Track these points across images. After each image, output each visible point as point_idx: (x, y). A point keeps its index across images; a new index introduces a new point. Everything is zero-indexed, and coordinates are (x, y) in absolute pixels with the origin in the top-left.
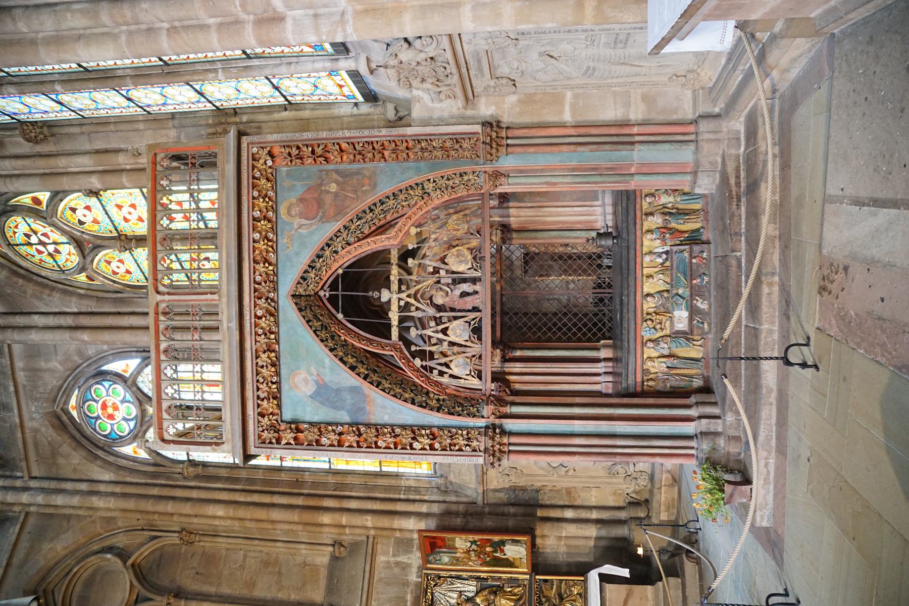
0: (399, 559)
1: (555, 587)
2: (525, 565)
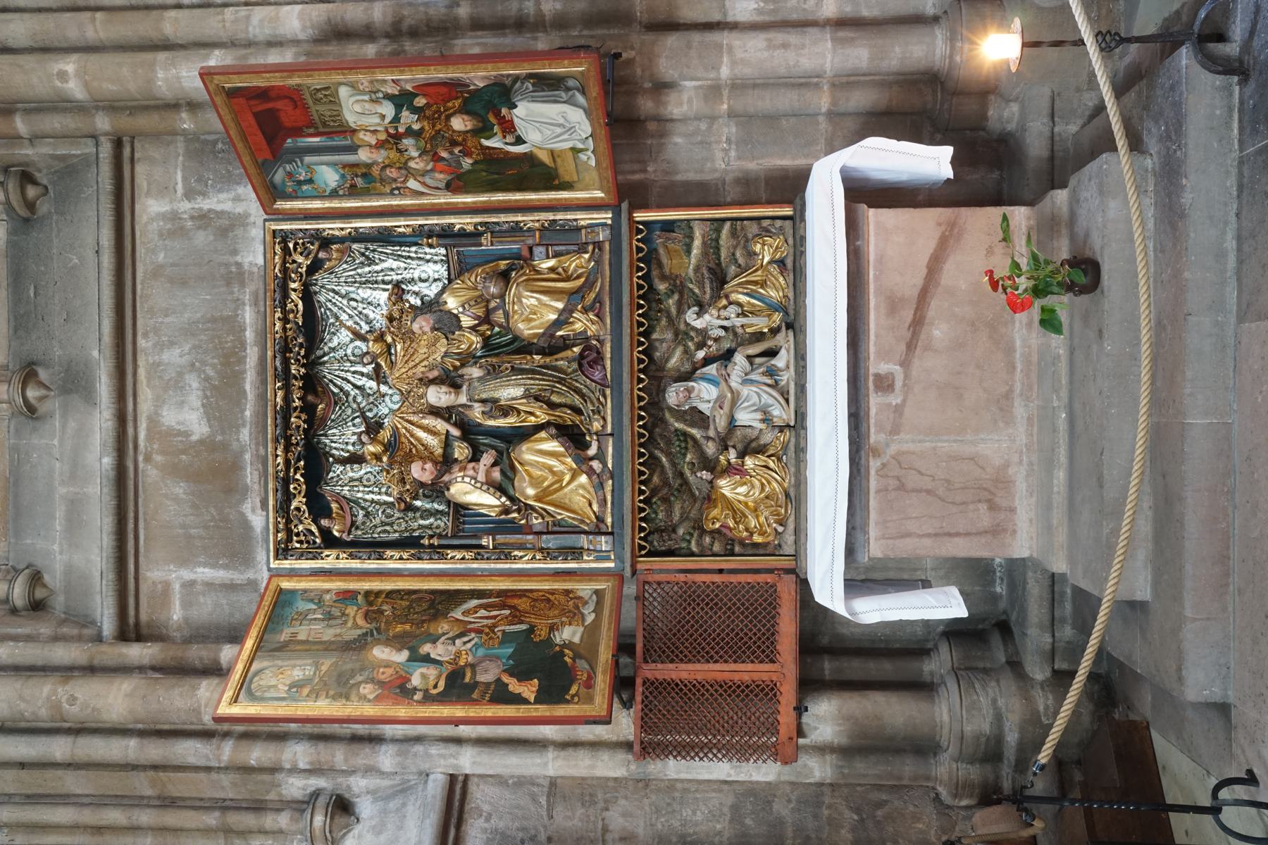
0: (206, 204)
1: (697, 243)
2: (595, 175)
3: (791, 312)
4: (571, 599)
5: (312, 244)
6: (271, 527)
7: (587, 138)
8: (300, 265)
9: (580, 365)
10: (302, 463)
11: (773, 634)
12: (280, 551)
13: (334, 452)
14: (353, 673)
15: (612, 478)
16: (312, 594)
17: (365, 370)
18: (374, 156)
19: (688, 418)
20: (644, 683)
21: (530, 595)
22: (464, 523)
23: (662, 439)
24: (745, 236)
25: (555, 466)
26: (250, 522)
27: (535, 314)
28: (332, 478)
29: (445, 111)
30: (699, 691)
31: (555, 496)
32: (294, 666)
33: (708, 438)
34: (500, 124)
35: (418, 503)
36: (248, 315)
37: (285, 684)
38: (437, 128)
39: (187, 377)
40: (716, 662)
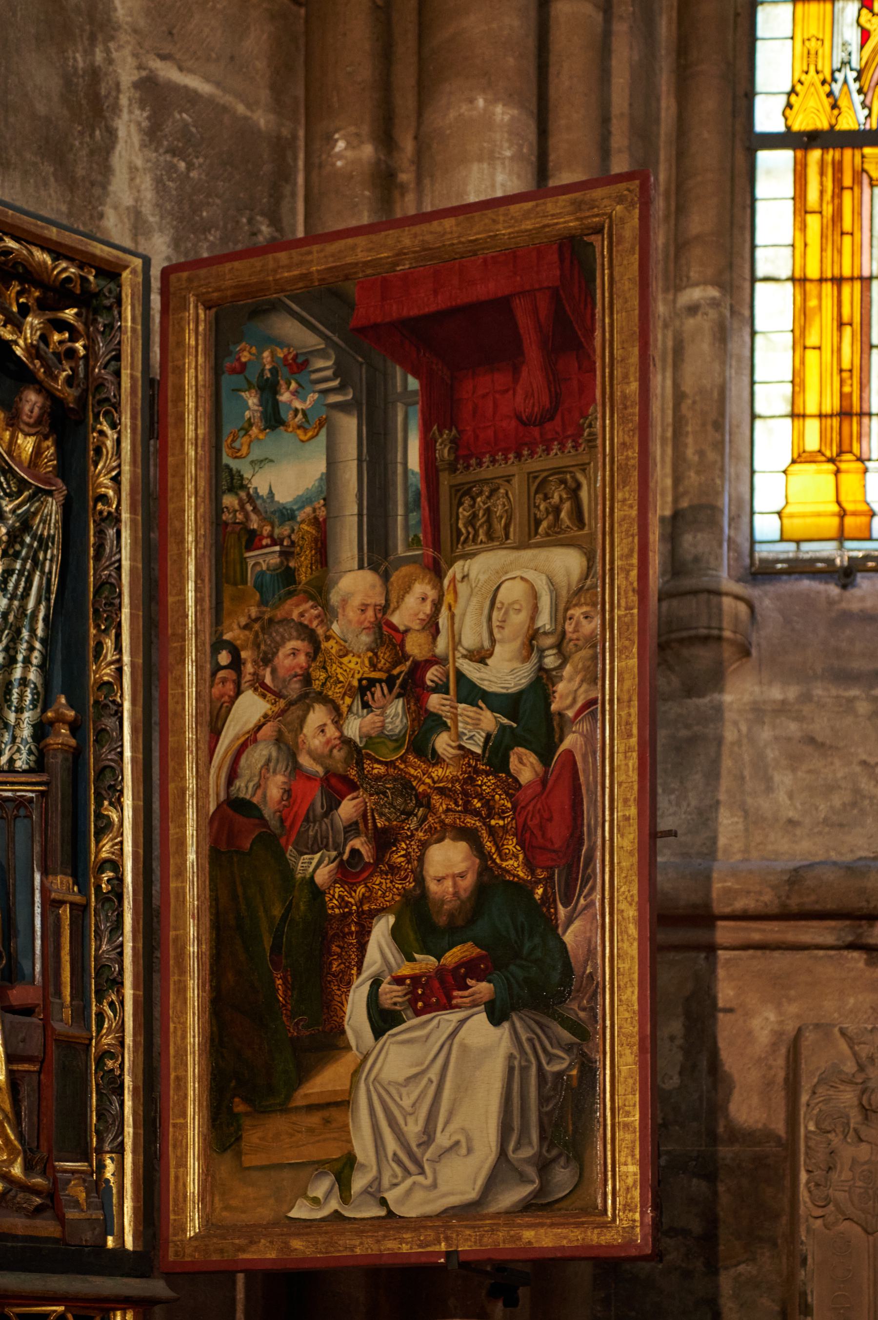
18: (352, 613)
34: (441, 971)
38: (436, 799)
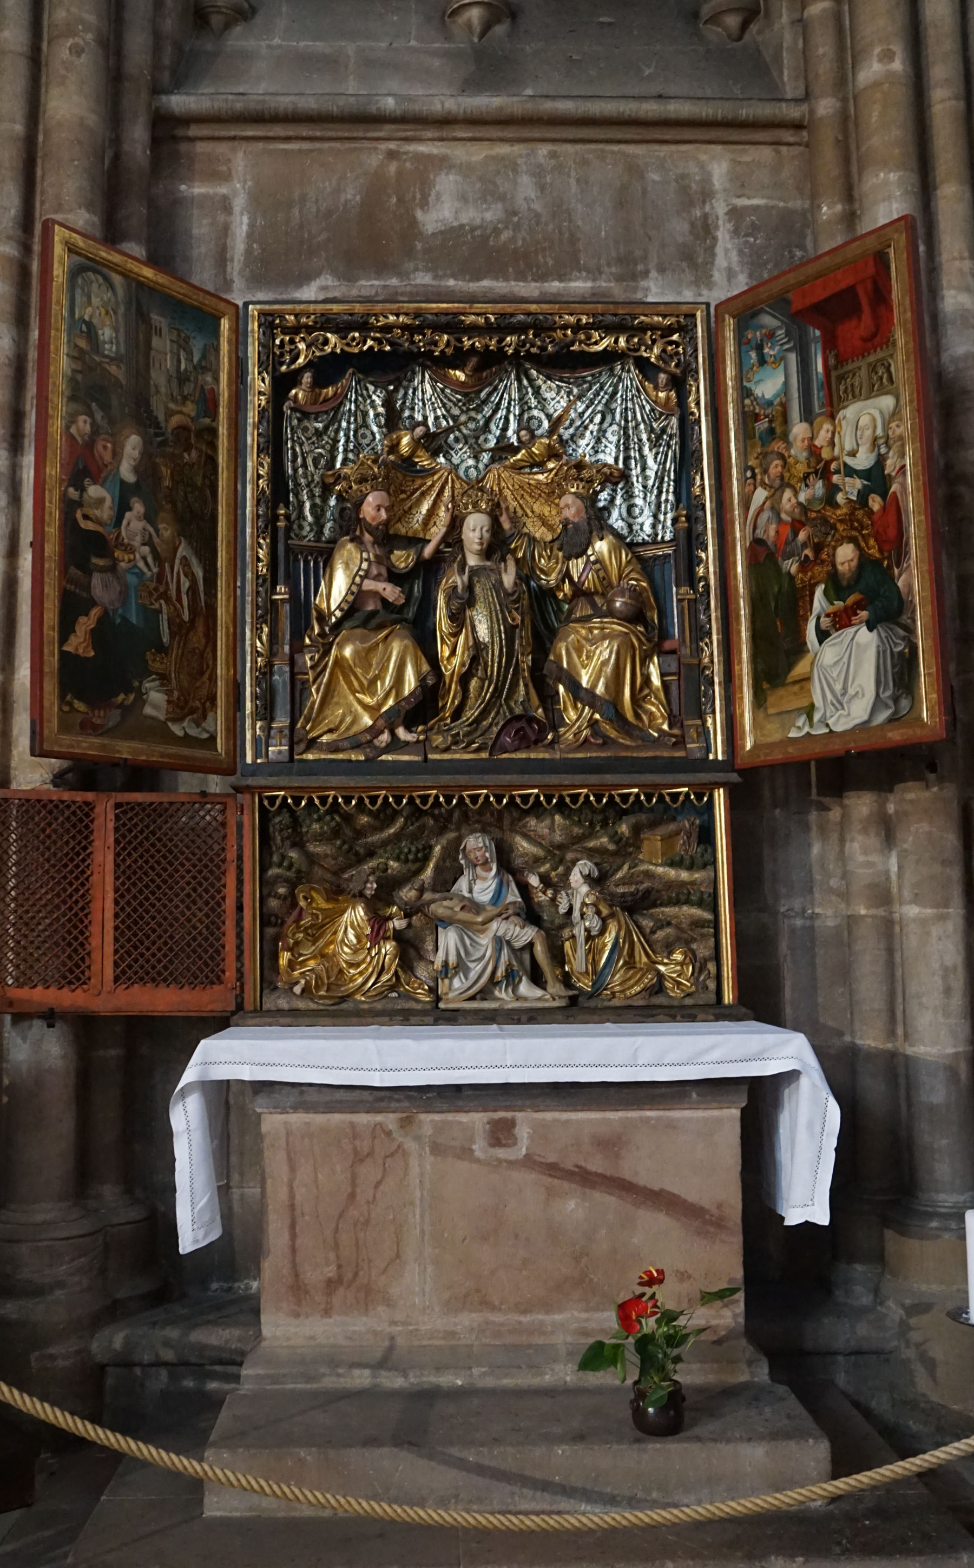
0: (723, 234)
1: (684, 875)
2: (776, 737)
3: (592, 1003)
4: (204, 704)
5: (677, 366)
6: (302, 307)
7: (827, 725)
8: (649, 348)
9: (518, 718)
10: (388, 348)
11: (154, 980)
12: (270, 319)
13: (402, 392)
14: (105, 407)
15: (367, 760)
16: (212, 358)
17: (510, 433)
18: (799, 443)
19: (448, 864)
20: (87, 803)
21: (209, 649)
22: (307, 563)
23: (419, 827)
24: (694, 940)
25: (383, 684)
26: (308, 285)
27: (588, 657)
28: (367, 389)
29: (863, 536)
30: (77, 878)
31: (342, 682)
32: (116, 330)
33: (422, 890)
34: (846, 609)
35: (333, 502)
36: (580, 285)
37: (91, 317)
38: (838, 525)
39: (500, 206)
40: (116, 903)
